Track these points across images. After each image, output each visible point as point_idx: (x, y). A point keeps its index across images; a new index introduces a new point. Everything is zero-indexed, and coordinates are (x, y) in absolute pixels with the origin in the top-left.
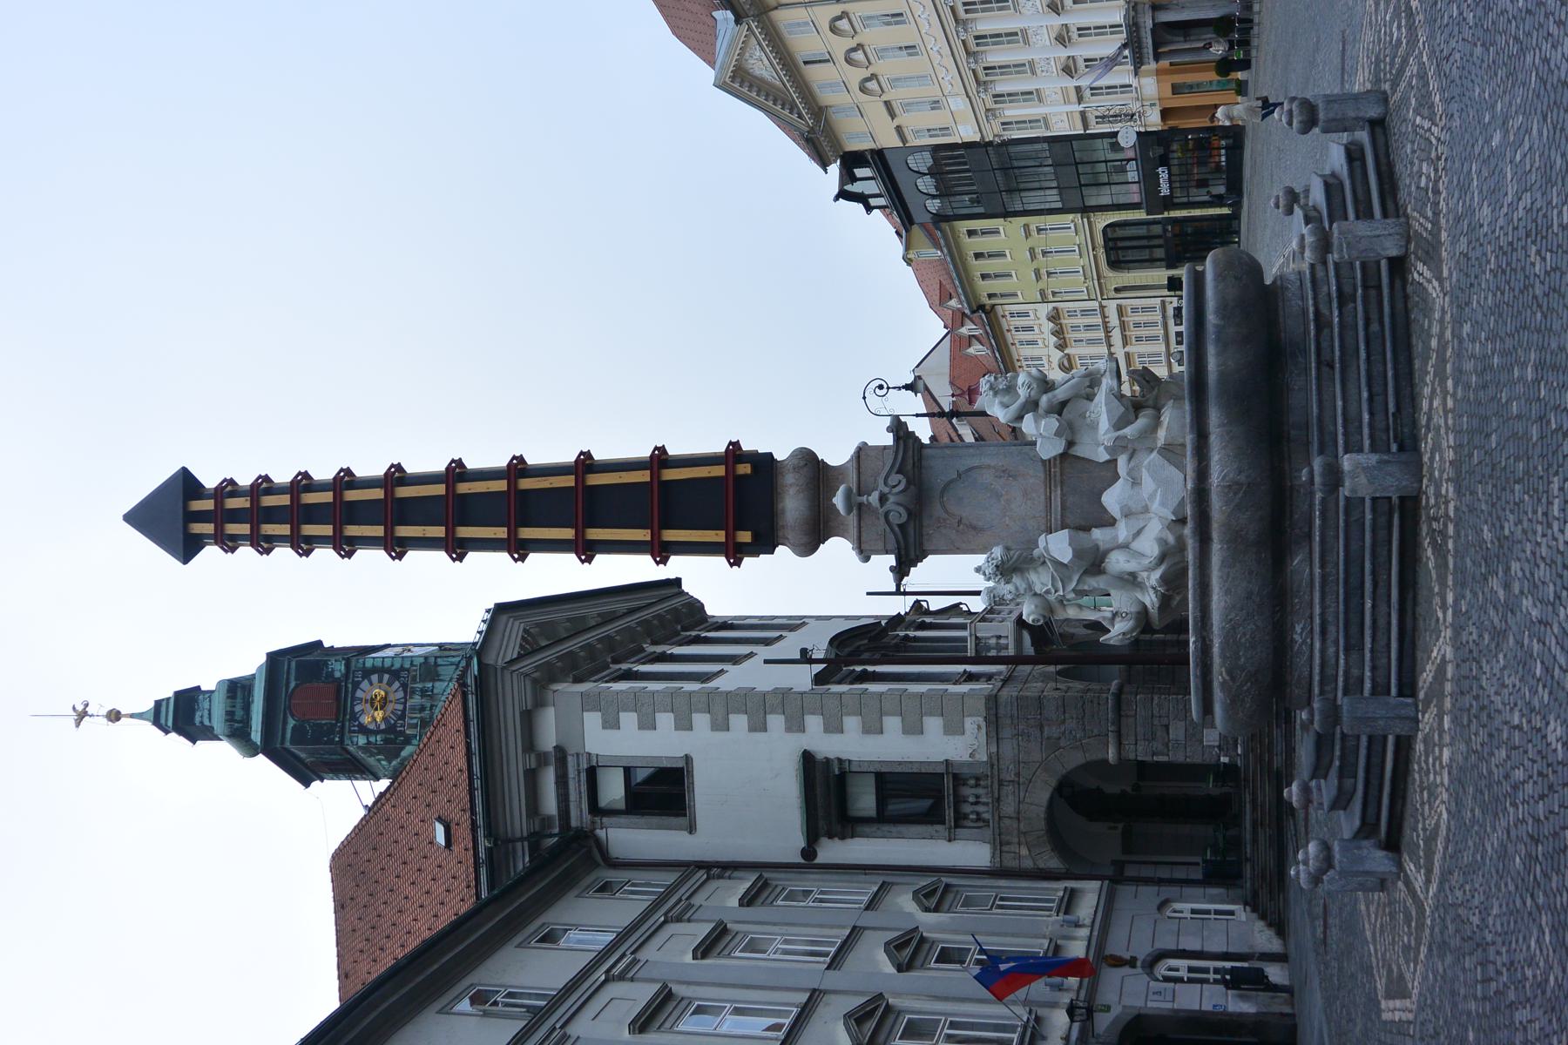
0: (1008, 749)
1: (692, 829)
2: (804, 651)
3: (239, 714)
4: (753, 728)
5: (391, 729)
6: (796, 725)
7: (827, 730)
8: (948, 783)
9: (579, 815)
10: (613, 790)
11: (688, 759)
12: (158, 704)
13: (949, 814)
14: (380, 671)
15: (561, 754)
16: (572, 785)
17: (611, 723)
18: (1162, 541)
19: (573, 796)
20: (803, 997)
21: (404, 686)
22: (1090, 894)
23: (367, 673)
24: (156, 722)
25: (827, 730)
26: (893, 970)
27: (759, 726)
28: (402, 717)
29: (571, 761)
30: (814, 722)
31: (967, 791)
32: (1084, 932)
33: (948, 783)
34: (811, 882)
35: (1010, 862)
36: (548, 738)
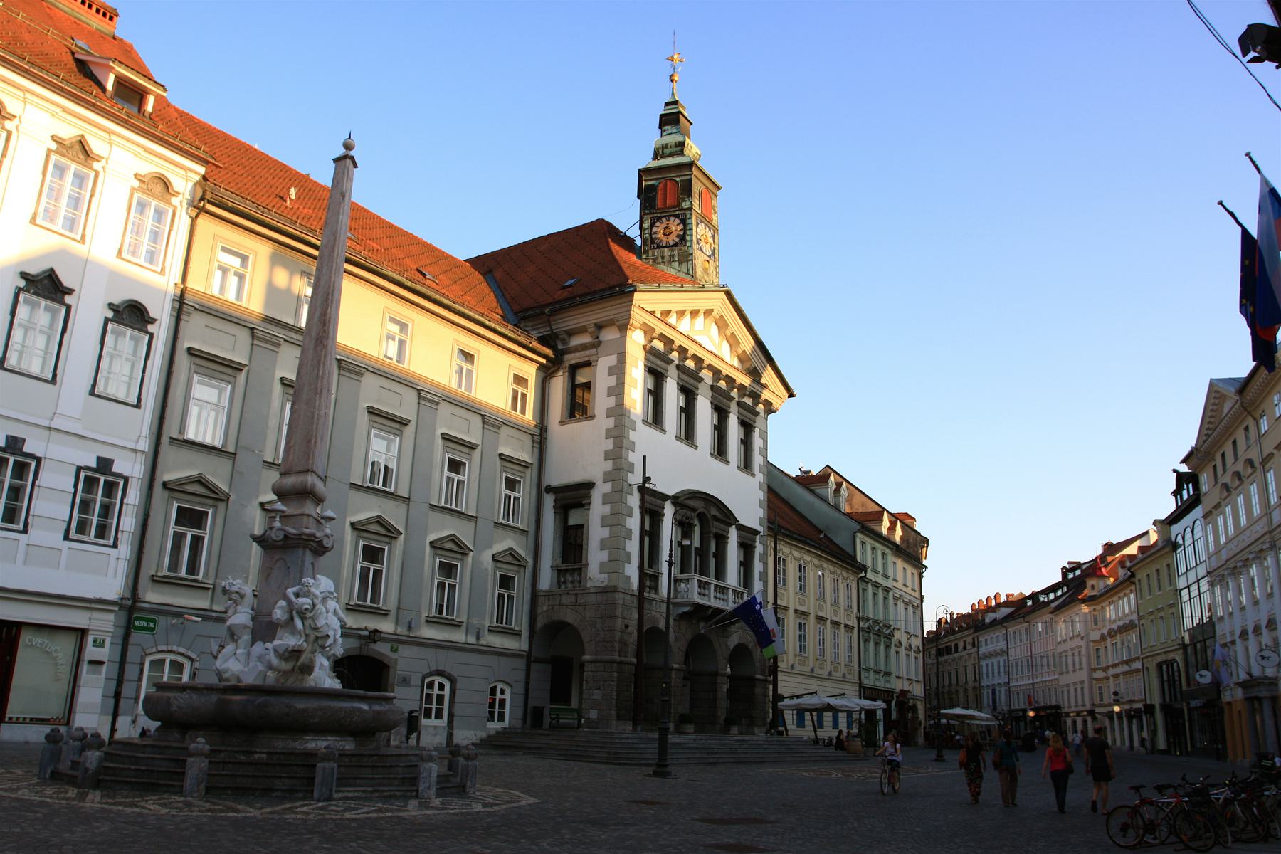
0: (591, 599)
1: (562, 423)
2: (649, 479)
3: (667, 151)
4: (606, 452)
5: (652, 241)
6: (608, 477)
7: (605, 496)
8: (576, 566)
9: (571, 359)
10: (581, 379)
11: (593, 417)
12: (676, 103)
13: (564, 567)
14: (684, 230)
15: (596, 344)
16: (582, 353)
17: (611, 371)
18: (227, 670)
19: (578, 354)
20: (403, 492)
21: (676, 245)
22: (522, 644)
23: (684, 222)
24: (667, 104)
25: (605, 496)
26: (432, 537)
27: (608, 456)
28: (659, 247)
29: (594, 351)
30: (607, 488)
31: (576, 577)
32: (472, 640)
33: (576, 566)
34: (525, 492)
35: (541, 600)
36: (609, 335)
